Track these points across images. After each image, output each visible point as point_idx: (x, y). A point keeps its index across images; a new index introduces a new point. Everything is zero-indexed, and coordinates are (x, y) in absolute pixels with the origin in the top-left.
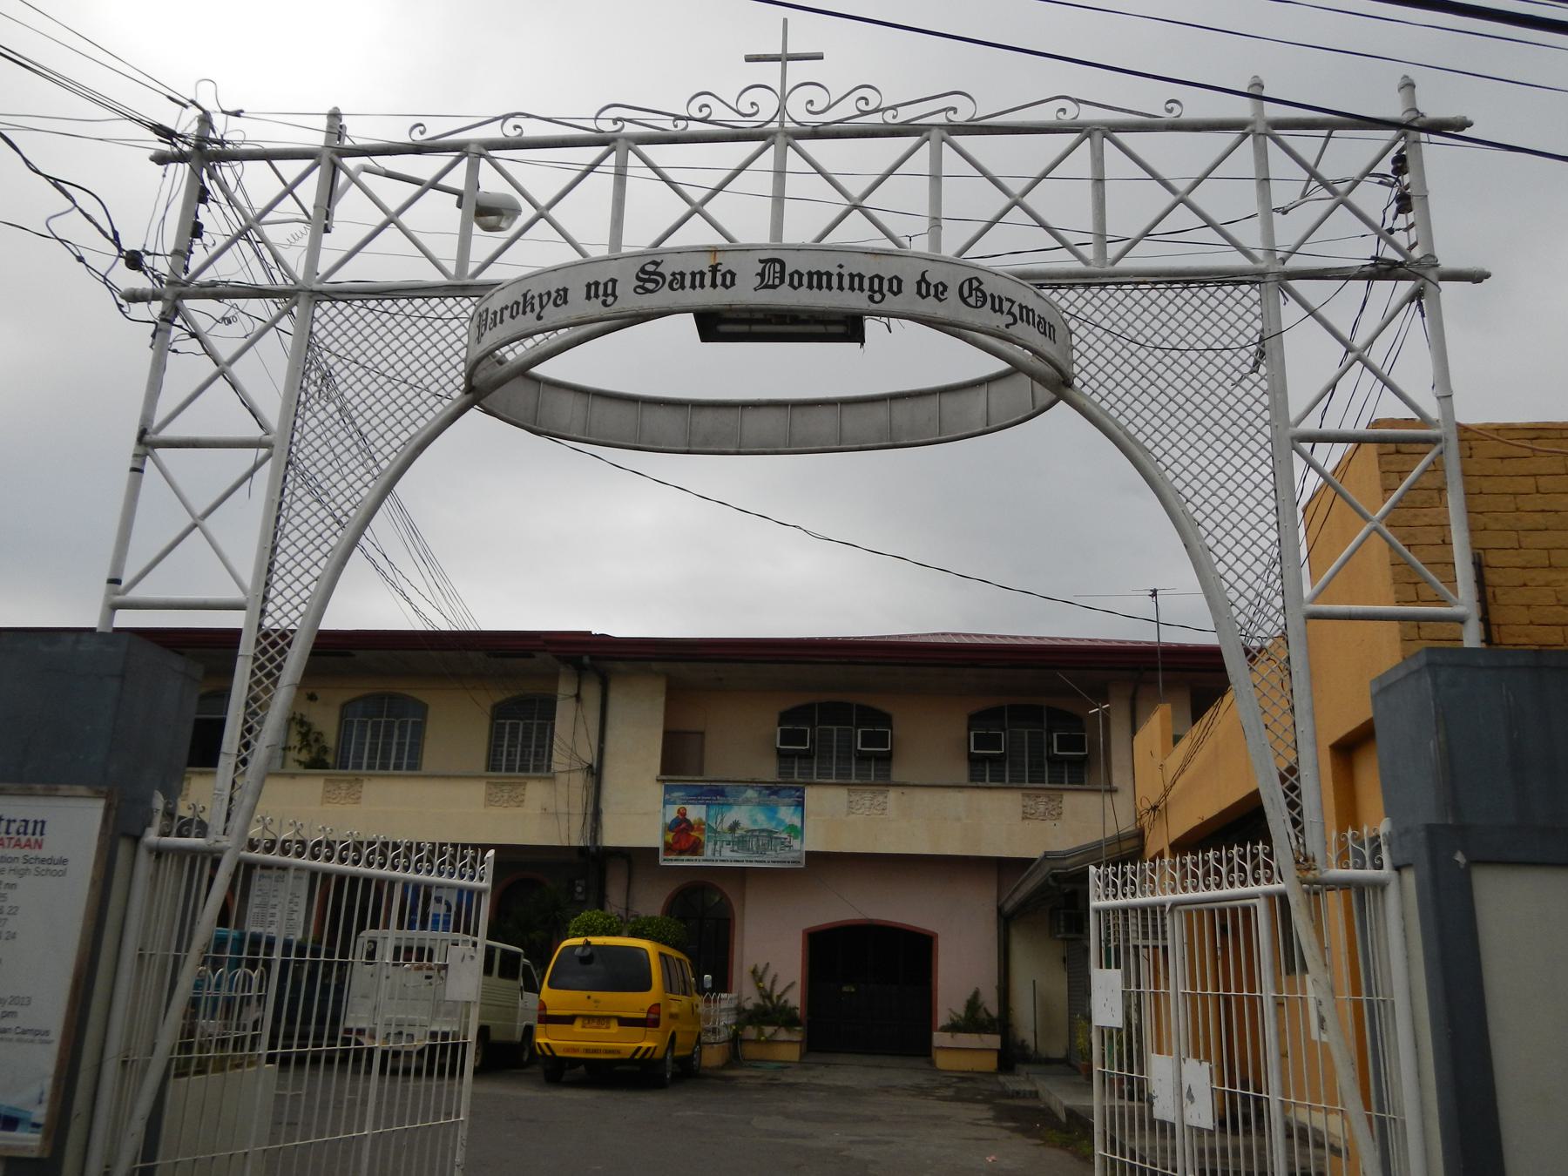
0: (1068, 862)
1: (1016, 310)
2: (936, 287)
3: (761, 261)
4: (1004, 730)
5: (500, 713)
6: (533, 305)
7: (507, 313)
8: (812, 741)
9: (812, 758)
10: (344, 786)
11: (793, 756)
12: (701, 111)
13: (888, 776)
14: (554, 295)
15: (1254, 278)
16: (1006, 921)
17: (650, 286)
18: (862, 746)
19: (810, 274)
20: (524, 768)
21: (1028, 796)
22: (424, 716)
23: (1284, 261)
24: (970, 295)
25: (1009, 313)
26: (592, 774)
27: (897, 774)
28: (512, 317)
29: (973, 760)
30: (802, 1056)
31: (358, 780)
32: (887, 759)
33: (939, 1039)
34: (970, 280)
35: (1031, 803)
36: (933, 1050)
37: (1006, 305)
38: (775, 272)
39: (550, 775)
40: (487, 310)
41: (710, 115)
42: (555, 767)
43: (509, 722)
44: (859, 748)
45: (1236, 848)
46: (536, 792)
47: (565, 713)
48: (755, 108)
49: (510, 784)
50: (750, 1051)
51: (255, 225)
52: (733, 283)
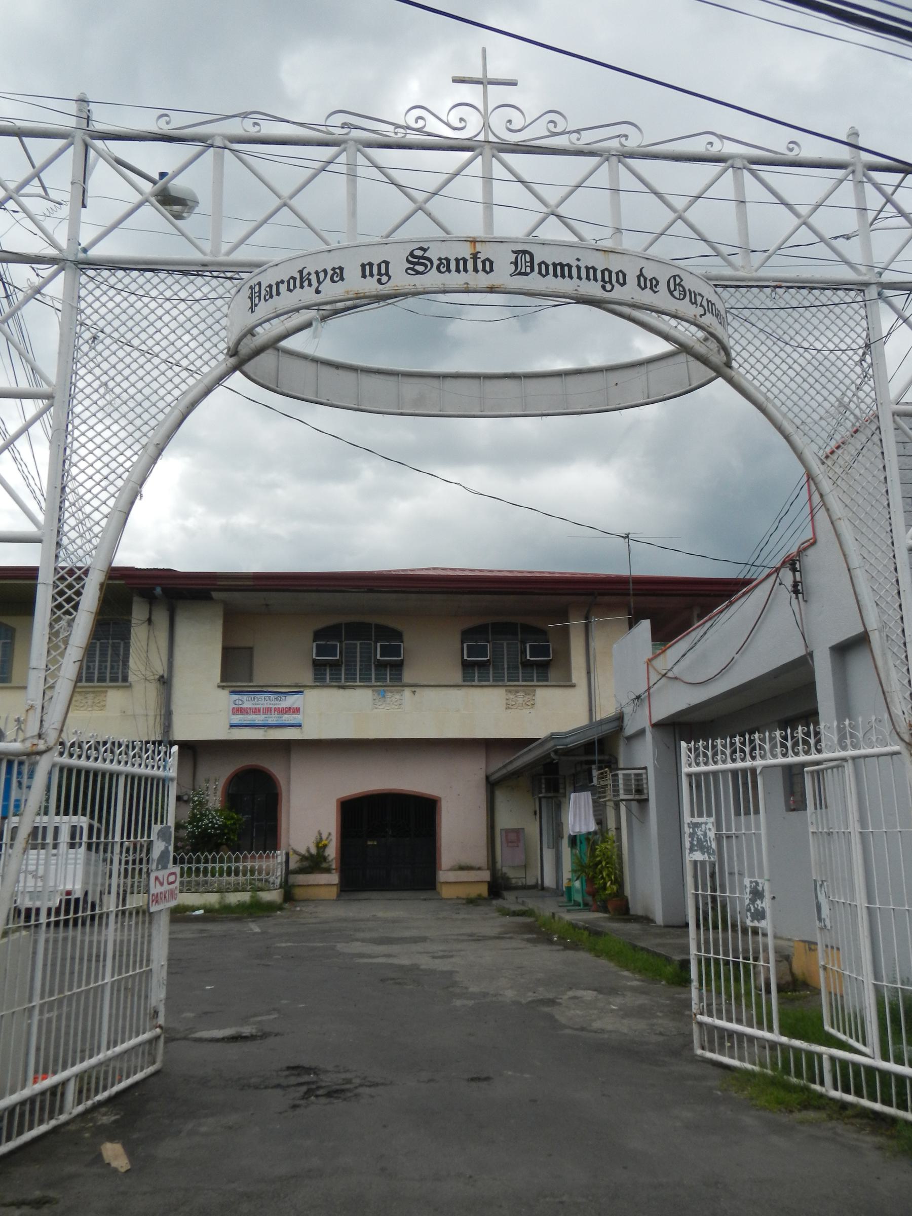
0: (568, 740)
1: (705, 303)
2: (651, 280)
3: (514, 252)
4: (488, 642)
6: (310, 281)
7: (283, 287)
9: (340, 666)
11: (325, 665)
12: (416, 122)
13: (400, 679)
14: (330, 273)
15: (861, 287)
16: (492, 785)
17: (420, 268)
18: (381, 657)
19: (555, 265)
20: (102, 679)
21: (510, 691)
22: (12, 638)
23: (880, 274)
24: (675, 289)
25: (701, 306)
26: (164, 683)
27: (408, 676)
28: (289, 290)
29: (467, 666)
30: (339, 896)
32: (398, 667)
33: (443, 876)
34: (674, 277)
35: (512, 697)
36: (438, 885)
37: (699, 299)
38: (526, 262)
40: (259, 284)
41: (424, 126)
42: (132, 678)
44: (378, 657)
45: (800, 728)
46: (115, 698)
47: (139, 634)
48: (463, 124)
49: (93, 692)
50: (298, 893)
51: (15, 196)
52: (492, 270)
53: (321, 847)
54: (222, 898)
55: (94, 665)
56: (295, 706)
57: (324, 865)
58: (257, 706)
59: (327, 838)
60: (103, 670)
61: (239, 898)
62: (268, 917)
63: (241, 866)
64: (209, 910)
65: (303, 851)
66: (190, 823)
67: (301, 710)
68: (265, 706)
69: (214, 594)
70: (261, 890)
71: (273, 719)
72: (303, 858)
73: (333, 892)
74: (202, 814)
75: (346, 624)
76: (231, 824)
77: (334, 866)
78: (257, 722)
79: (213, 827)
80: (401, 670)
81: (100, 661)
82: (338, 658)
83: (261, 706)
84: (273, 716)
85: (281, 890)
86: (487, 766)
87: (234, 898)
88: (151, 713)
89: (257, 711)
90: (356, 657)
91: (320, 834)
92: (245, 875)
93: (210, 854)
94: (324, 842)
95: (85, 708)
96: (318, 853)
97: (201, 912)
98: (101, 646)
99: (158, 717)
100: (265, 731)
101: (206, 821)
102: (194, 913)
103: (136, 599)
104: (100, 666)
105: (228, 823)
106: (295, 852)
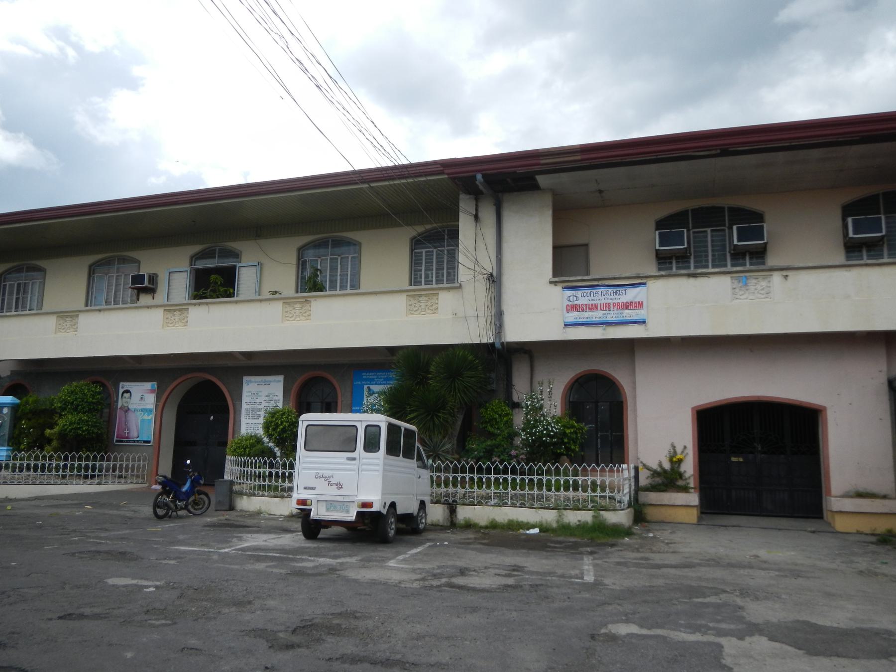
5: (416, 243)
8: (689, 243)
9: (689, 257)
10: (298, 306)
11: (671, 258)
18: (739, 241)
26: (493, 281)
30: (700, 519)
31: (307, 301)
32: (759, 255)
33: (835, 502)
36: (825, 514)
39: (456, 285)
43: (424, 251)
44: (735, 242)
46: (446, 299)
49: (426, 295)
50: (651, 513)
53: (676, 463)
54: (560, 516)
55: (432, 274)
56: (637, 300)
57: (680, 483)
58: (594, 302)
59: (683, 452)
60: (440, 278)
61: (579, 518)
62: (612, 545)
63: (580, 479)
64: (544, 529)
65: (655, 466)
66: (523, 430)
67: (645, 304)
68: (603, 301)
69: (541, 180)
70: (605, 509)
71: (612, 316)
72: (655, 474)
73: (692, 516)
74: (536, 421)
75: (693, 210)
76: (571, 433)
77: (692, 485)
78: (594, 319)
79: (548, 435)
80: (764, 259)
81: (437, 269)
82: (686, 246)
83: (598, 302)
84: (612, 312)
85: (631, 510)
86: (889, 370)
87: (573, 517)
88: (482, 314)
89: (594, 308)
90: (707, 246)
91: (674, 447)
92: (585, 491)
93: (553, 465)
94: (679, 456)
95: (418, 312)
96: (672, 469)
97: (536, 531)
98: (437, 255)
99: (489, 318)
100: (604, 329)
101: (540, 428)
102: (528, 532)
103: (462, 196)
104: (437, 273)
105: (568, 431)
106: (645, 466)
